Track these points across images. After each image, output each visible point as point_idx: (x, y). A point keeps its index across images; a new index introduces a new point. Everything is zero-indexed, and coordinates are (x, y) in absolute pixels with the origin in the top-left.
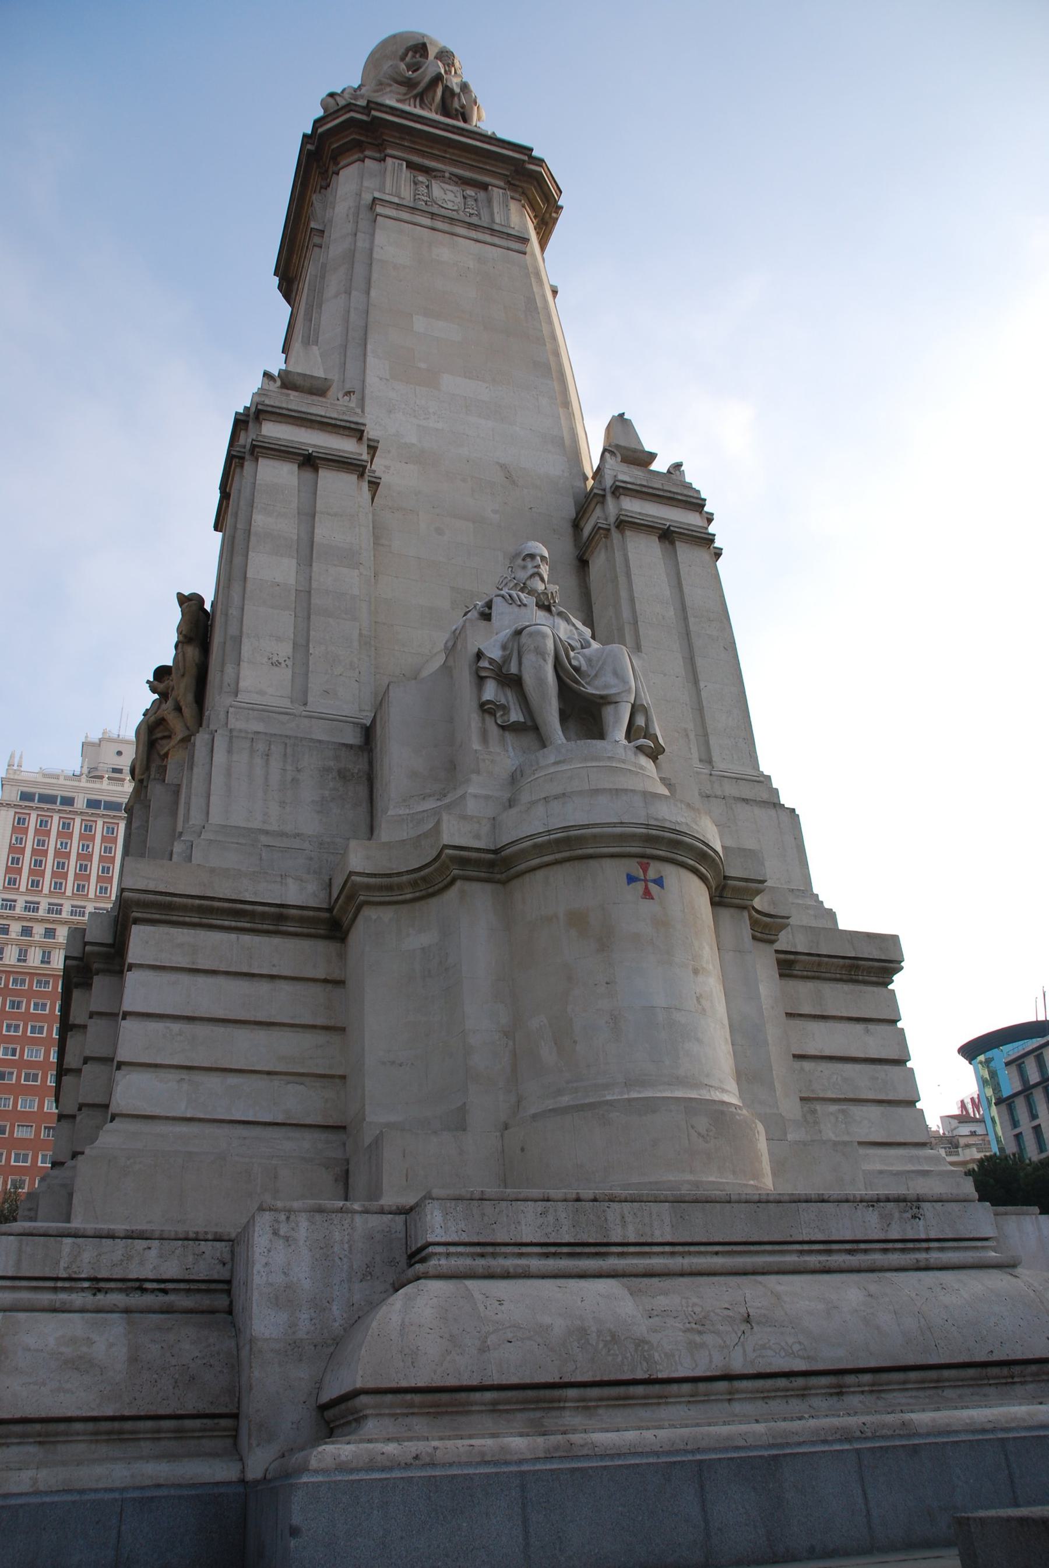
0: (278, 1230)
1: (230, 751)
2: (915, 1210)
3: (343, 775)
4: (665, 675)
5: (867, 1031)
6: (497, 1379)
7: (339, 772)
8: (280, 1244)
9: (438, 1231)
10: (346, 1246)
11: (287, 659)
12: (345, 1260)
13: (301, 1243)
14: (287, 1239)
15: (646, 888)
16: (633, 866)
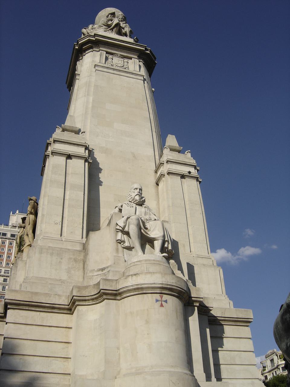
1: (41, 253)
3: (76, 260)
4: (180, 223)
7: (74, 259)
15: (162, 303)
16: (158, 296)
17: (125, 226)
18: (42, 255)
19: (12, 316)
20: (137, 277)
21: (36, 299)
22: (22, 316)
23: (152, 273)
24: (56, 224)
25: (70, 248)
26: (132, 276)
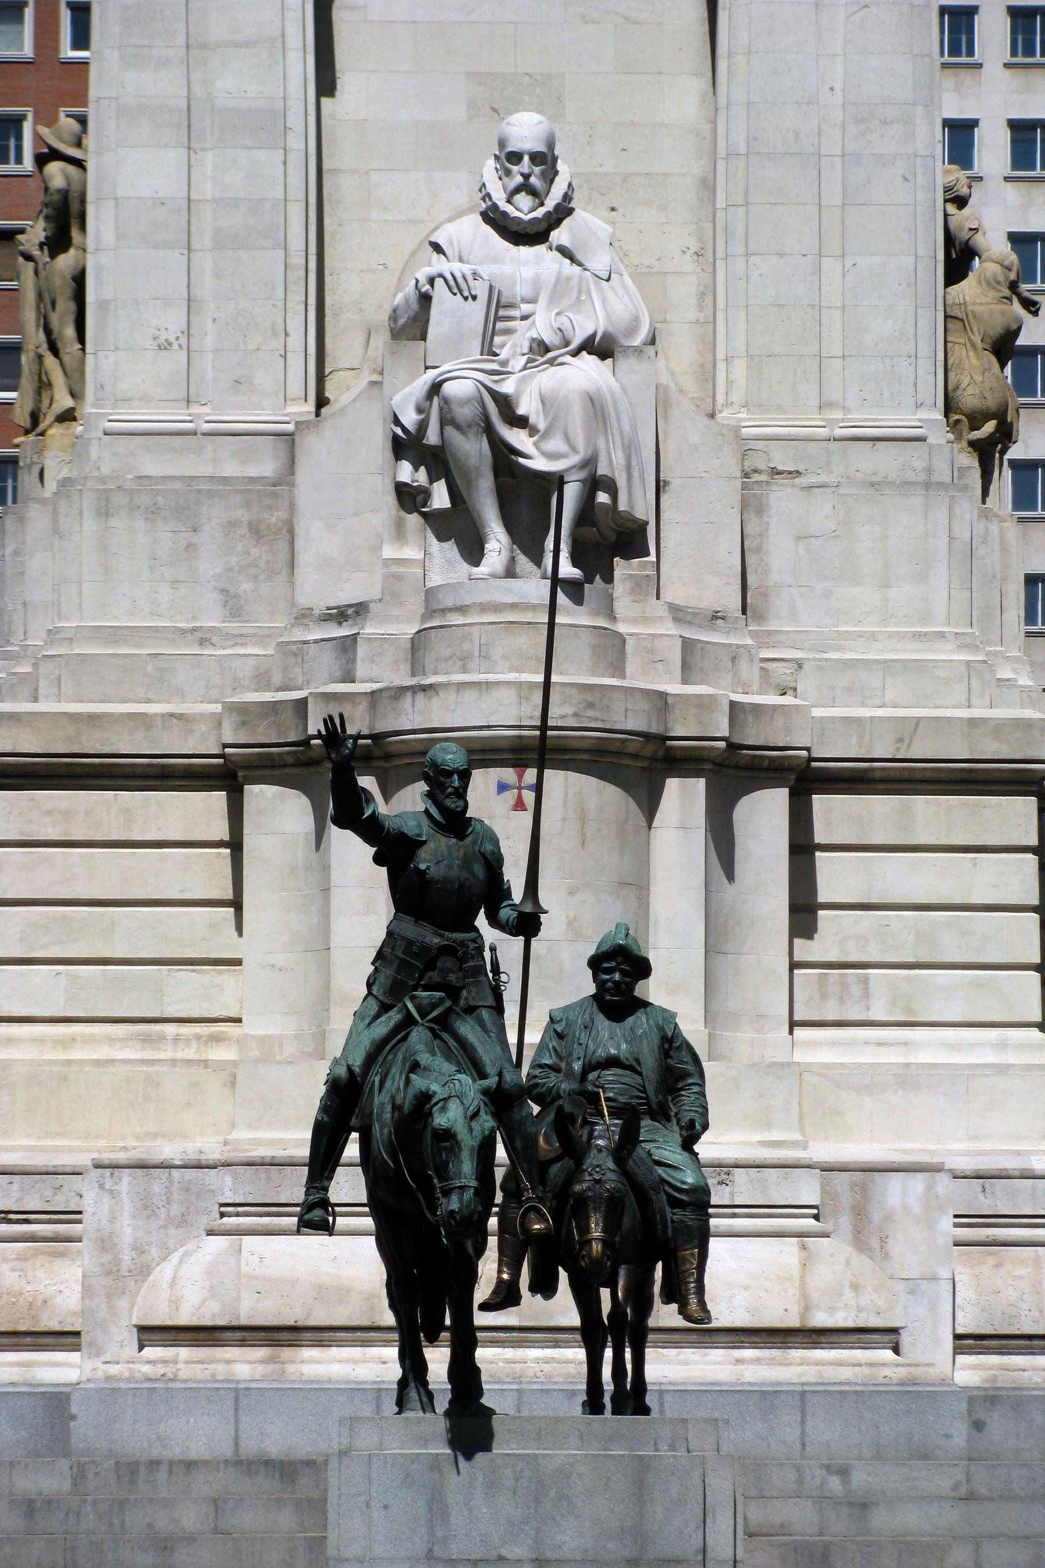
0: (104, 1184)
1: (105, 512)
2: (724, 1177)
3: (256, 531)
4: (782, 255)
5: (975, 863)
6: (244, 1321)
7: (250, 525)
8: (106, 1197)
9: (228, 1193)
10: (164, 1198)
11: (179, 334)
12: (163, 1209)
13: (124, 1195)
14: (111, 1192)
15: (520, 797)
17: (422, 426)
18: (113, 522)
19: (11, 813)
20: (430, 698)
21: (94, 742)
22: (48, 813)
23: (484, 687)
24: (165, 346)
25: (231, 469)
26: (414, 693)
